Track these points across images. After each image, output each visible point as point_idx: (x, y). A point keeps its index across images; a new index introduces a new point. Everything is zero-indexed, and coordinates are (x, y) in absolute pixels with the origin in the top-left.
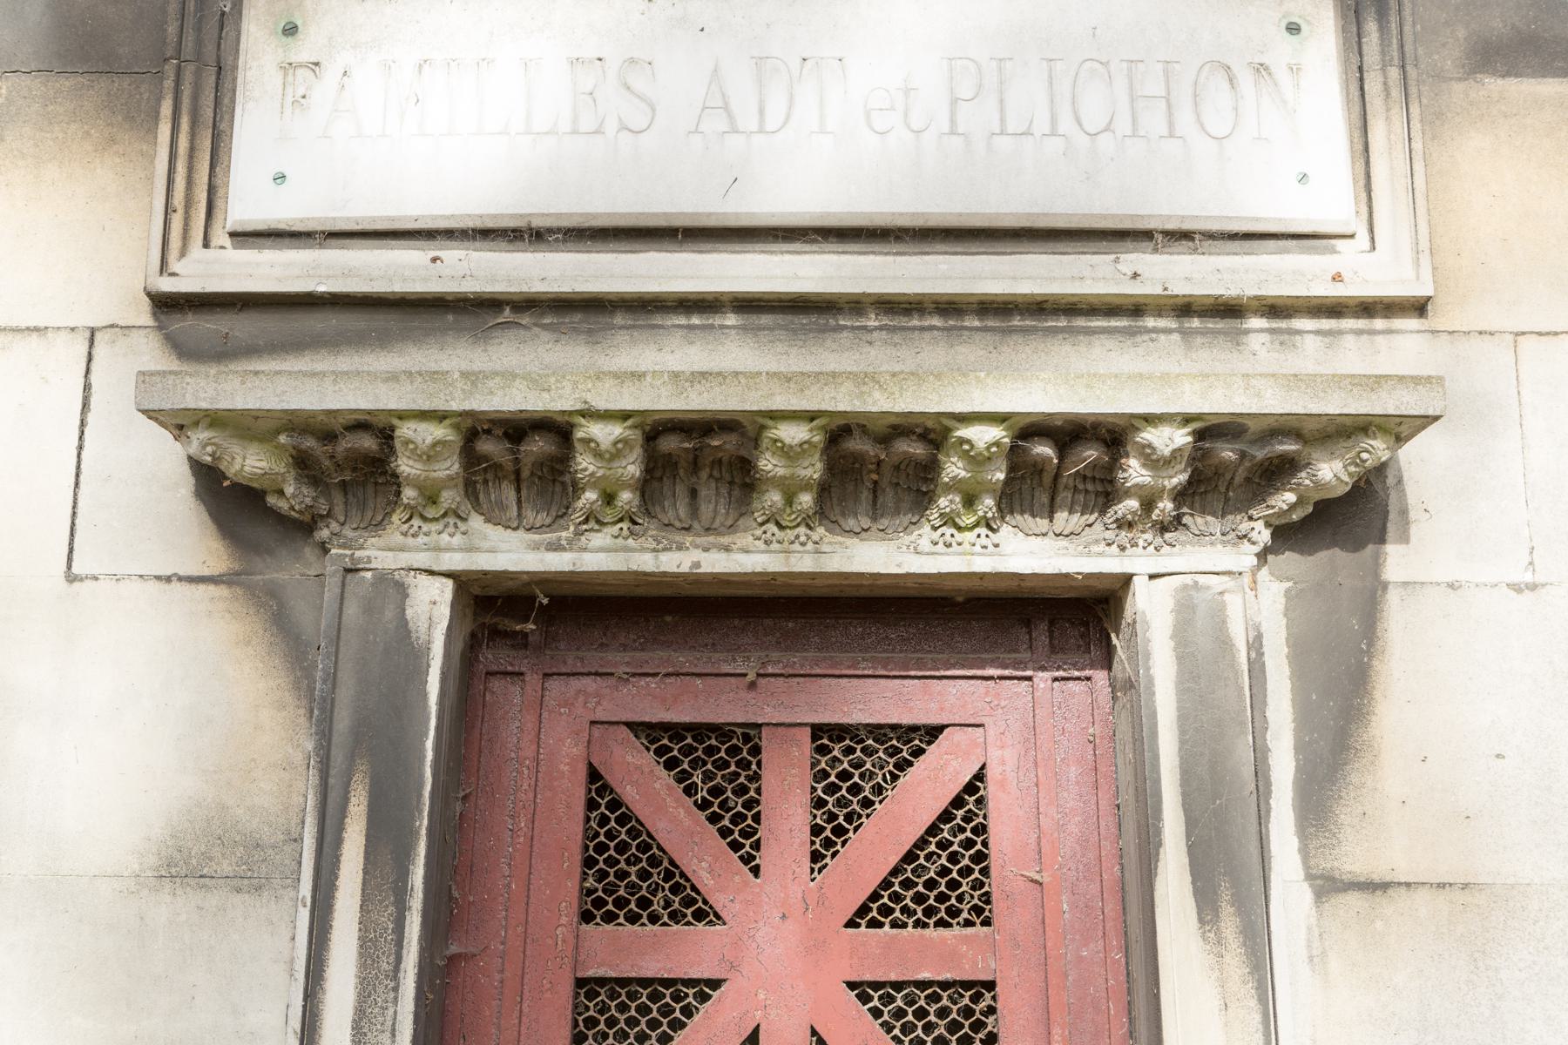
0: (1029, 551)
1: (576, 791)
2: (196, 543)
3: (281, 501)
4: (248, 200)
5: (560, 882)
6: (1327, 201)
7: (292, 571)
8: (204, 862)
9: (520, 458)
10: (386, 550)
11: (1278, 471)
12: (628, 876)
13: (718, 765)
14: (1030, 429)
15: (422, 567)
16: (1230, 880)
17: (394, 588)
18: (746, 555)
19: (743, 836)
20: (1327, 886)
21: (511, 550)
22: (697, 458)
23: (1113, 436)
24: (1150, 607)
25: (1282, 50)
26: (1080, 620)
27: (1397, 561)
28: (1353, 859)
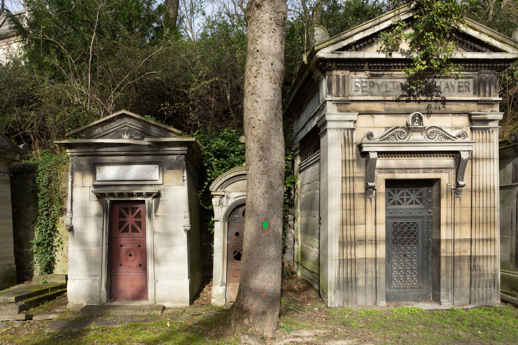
0: (140, 199)
1: (118, 211)
2: (96, 199)
3: (100, 197)
4: (98, 179)
5: (118, 216)
6: (157, 178)
7: (101, 200)
8: (98, 215)
9: (112, 195)
10: (106, 199)
11: (152, 195)
12: (122, 216)
13: (126, 209)
14: (137, 193)
15: (108, 200)
16: (150, 216)
17: (106, 201)
18: (125, 199)
19: (128, 213)
20: (156, 216)
21: (112, 199)
22: (121, 195)
23: (142, 193)
24: (146, 202)
25: (155, 169)
26: (143, 202)
27: (160, 199)
28: (157, 214)
